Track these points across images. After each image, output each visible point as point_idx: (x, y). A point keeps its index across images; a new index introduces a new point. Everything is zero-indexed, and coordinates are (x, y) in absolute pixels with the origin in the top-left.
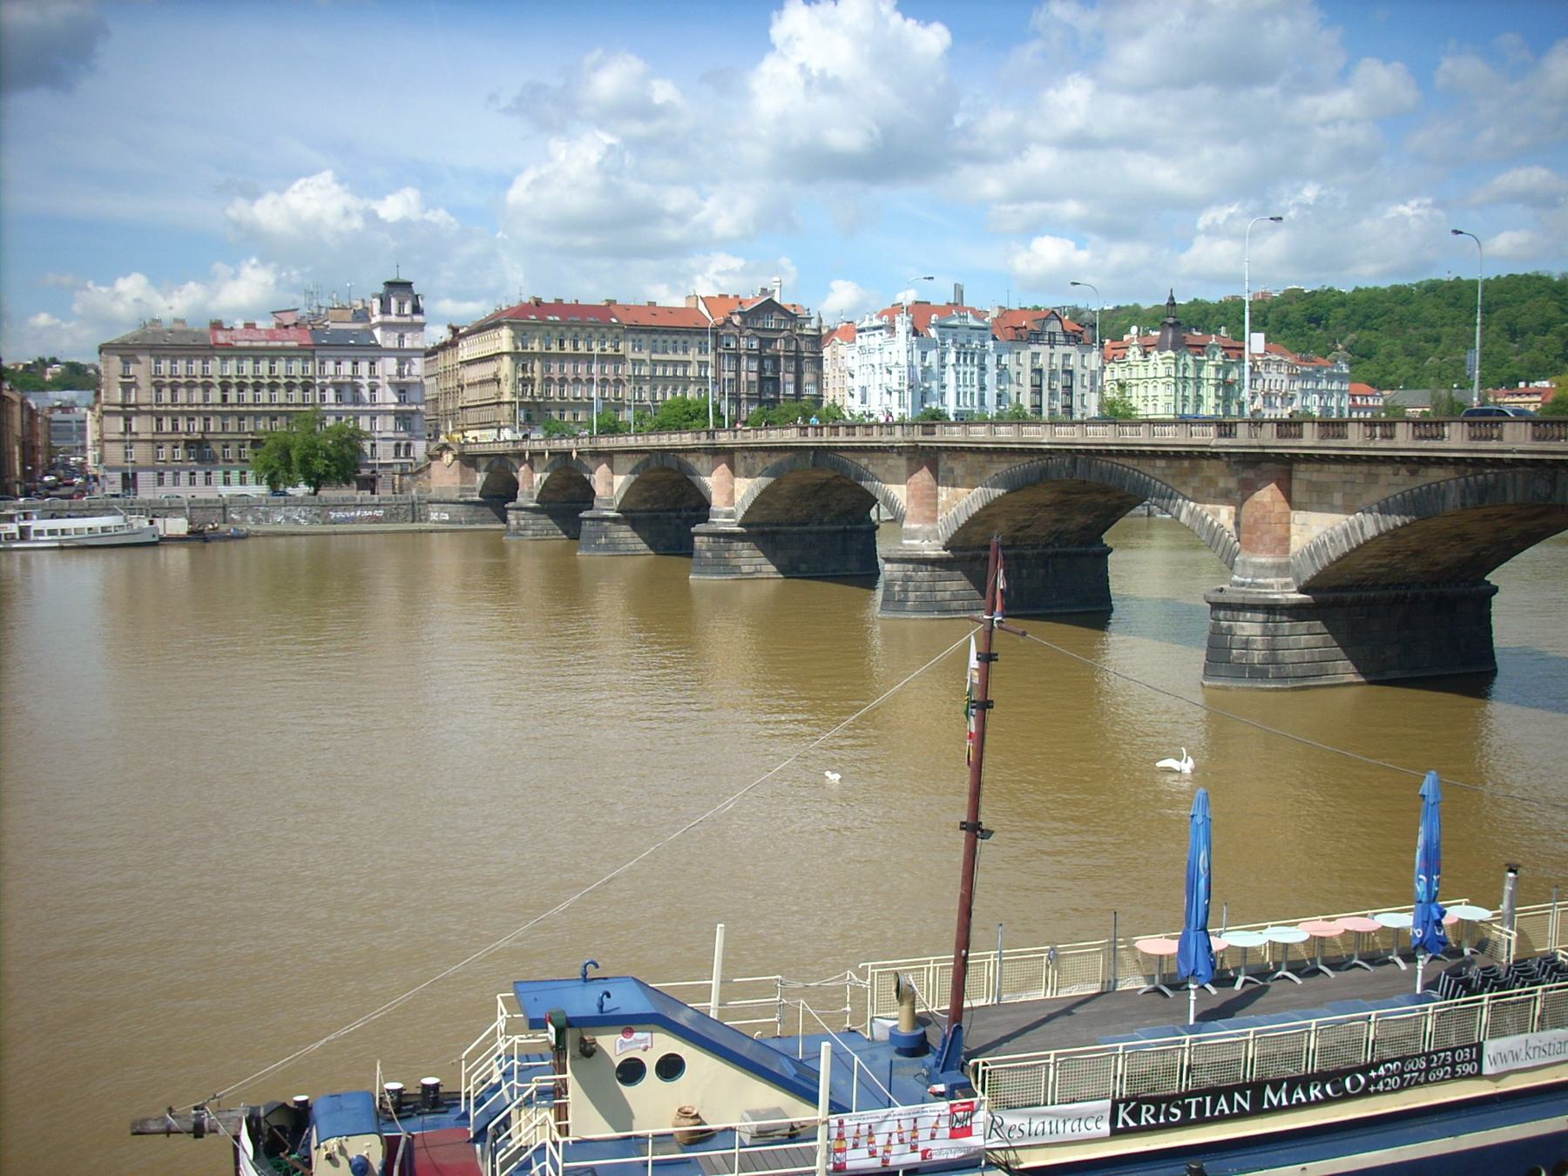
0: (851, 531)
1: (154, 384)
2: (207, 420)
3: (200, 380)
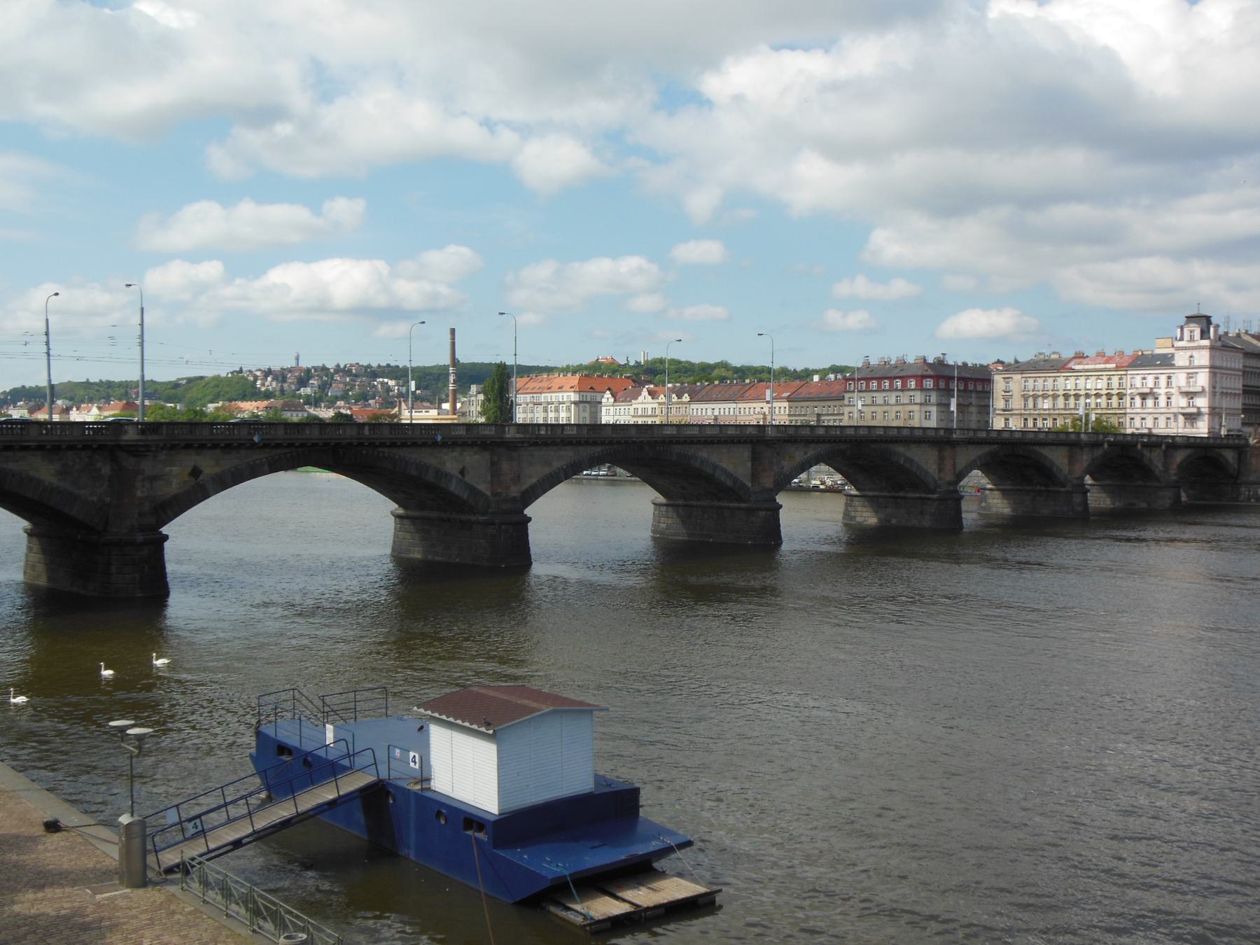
0: (925, 499)
1: (1023, 396)
2: (1055, 419)
3: (1051, 393)
